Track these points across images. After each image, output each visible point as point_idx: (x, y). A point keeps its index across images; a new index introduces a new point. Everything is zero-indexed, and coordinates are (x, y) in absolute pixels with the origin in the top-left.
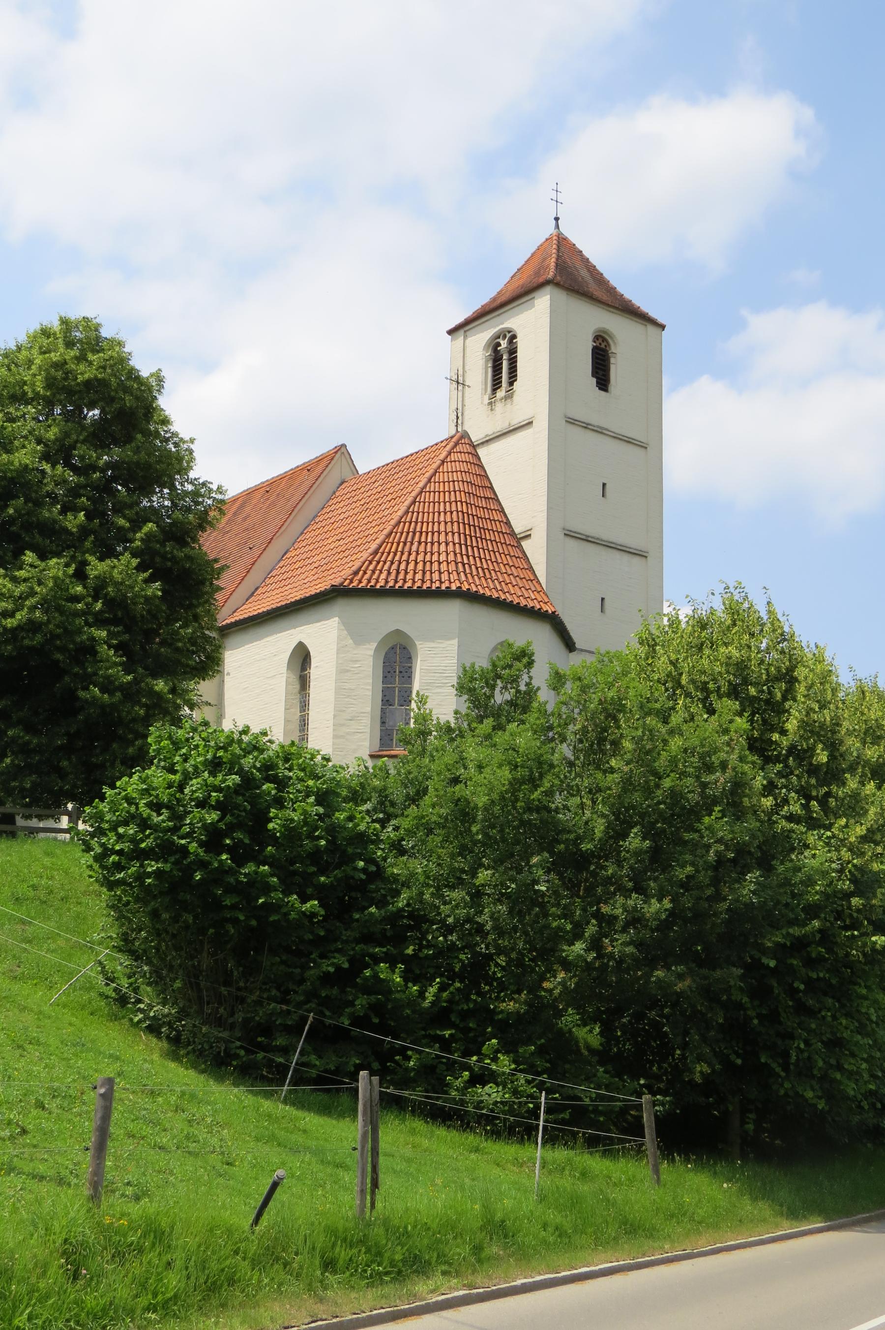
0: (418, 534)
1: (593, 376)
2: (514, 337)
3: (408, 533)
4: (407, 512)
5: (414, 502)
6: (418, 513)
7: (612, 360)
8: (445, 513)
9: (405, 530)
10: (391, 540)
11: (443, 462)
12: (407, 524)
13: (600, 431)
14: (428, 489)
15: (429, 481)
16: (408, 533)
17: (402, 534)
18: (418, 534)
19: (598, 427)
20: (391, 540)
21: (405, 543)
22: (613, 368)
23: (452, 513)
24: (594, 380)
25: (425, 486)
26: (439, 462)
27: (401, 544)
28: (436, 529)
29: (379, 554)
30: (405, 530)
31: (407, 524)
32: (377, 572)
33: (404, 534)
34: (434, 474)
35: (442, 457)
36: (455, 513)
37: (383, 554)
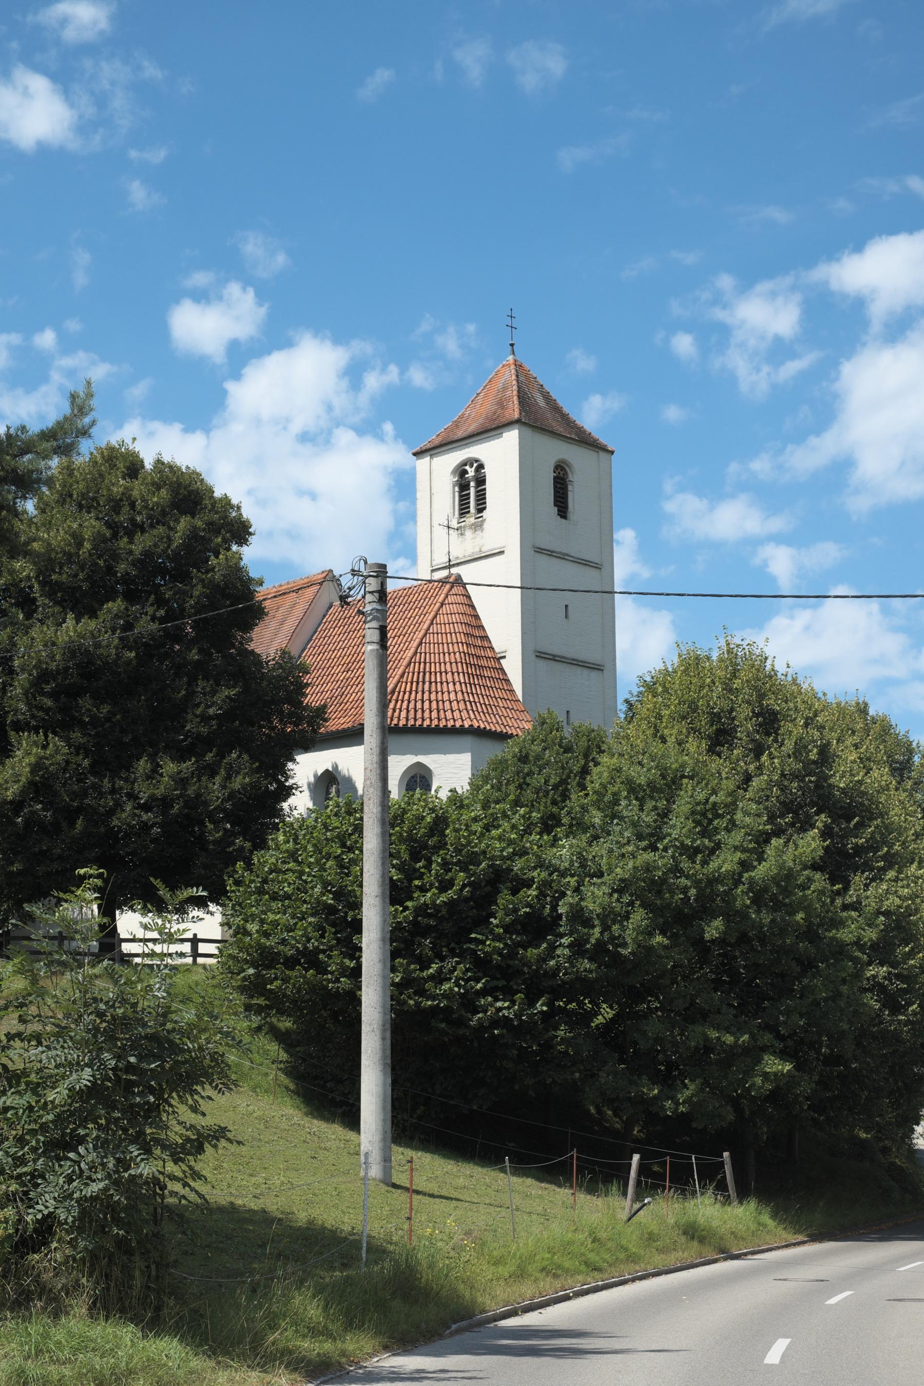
0: (427, 674)
1: (555, 505)
3: (419, 673)
4: (415, 653)
5: (420, 643)
6: (426, 653)
7: (570, 488)
9: (416, 670)
10: (404, 680)
12: (417, 664)
13: (563, 556)
14: (431, 631)
15: (432, 623)
16: (419, 673)
17: (413, 673)
18: (427, 674)
19: (560, 553)
20: (404, 680)
21: (418, 683)
22: (570, 494)
24: (556, 508)
25: (428, 629)
27: (414, 684)
28: (443, 670)
29: (396, 693)
30: (416, 670)
31: (417, 664)
32: (398, 711)
33: (416, 674)
34: (435, 617)
37: (399, 693)
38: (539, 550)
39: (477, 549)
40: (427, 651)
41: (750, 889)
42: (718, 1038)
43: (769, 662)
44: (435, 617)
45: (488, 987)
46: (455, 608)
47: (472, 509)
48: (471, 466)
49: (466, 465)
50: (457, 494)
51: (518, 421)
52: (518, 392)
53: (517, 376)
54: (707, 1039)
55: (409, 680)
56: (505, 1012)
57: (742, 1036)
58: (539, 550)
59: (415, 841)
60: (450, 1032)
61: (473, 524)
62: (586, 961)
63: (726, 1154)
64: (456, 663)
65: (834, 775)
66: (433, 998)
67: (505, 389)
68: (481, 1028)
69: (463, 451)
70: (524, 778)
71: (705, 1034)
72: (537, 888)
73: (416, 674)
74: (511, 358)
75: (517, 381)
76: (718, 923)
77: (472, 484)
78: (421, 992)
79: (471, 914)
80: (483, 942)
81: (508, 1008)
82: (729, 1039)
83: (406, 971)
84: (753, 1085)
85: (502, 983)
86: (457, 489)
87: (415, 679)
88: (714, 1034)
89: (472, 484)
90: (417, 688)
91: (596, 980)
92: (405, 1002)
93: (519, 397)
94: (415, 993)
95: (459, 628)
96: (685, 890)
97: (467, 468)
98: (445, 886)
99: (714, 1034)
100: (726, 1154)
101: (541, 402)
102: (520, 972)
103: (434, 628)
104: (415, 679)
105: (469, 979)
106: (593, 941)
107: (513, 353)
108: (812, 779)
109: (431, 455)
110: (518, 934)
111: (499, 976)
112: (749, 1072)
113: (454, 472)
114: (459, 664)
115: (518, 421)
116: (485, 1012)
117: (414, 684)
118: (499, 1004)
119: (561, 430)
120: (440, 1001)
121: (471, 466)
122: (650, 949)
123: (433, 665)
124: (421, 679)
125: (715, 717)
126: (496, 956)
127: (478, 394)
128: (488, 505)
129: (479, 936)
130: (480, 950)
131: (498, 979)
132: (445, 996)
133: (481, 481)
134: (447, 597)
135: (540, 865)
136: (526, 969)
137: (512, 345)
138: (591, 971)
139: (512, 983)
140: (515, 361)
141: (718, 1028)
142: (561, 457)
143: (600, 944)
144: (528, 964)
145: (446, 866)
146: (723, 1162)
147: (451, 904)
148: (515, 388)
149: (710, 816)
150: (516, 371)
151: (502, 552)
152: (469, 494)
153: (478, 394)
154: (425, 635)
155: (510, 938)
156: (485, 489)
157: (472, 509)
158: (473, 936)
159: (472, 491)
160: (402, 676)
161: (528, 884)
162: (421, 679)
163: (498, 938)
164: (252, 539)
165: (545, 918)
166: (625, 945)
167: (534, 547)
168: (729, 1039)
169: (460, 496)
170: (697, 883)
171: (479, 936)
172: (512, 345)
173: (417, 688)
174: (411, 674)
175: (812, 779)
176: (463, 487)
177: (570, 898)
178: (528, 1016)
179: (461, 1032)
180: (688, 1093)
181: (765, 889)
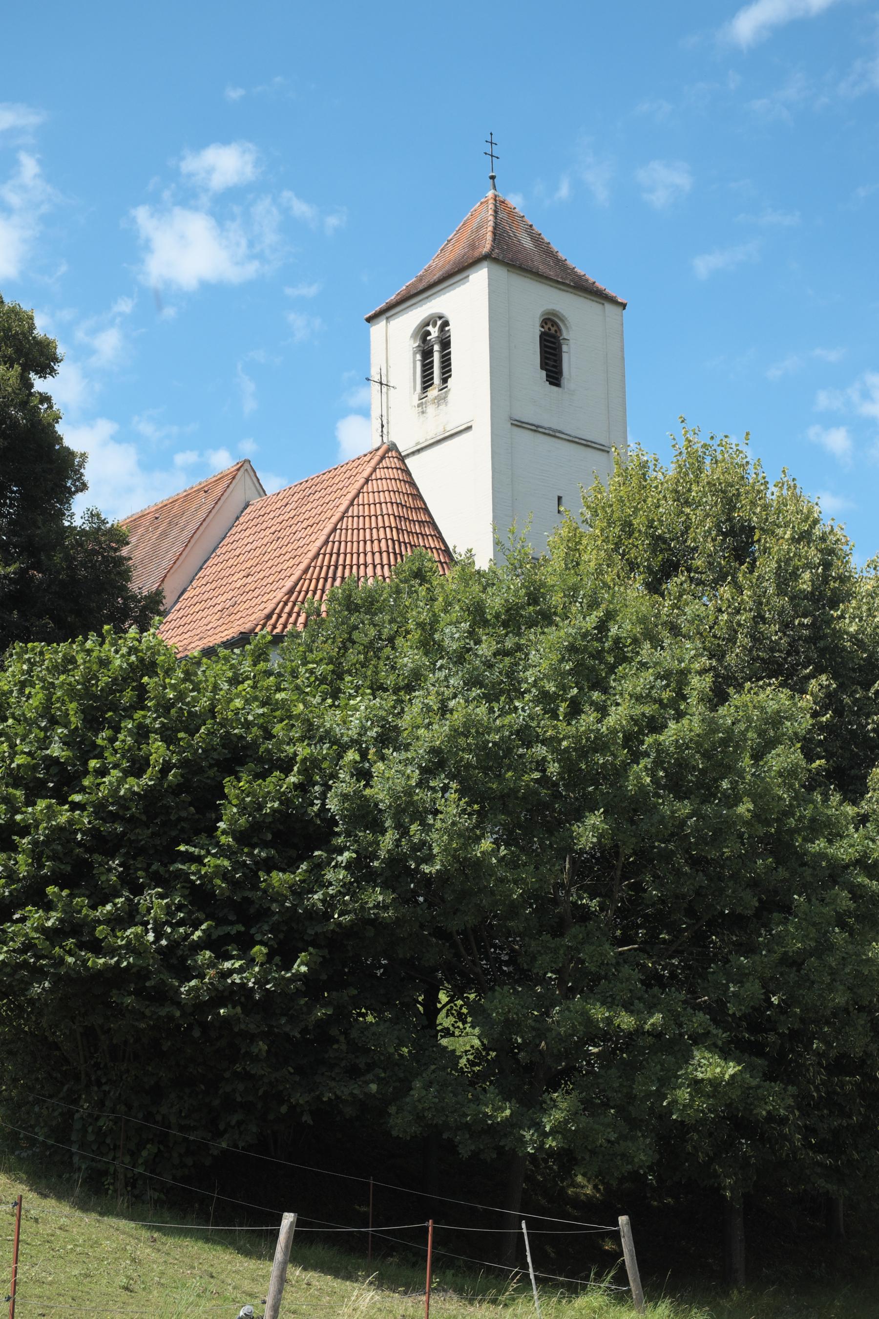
0: (340, 568)
1: (542, 368)
2: (446, 323)
3: (329, 567)
4: (326, 542)
5: (334, 530)
6: (340, 542)
8: (372, 542)
9: (326, 563)
10: (308, 576)
11: (367, 480)
12: (327, 556)
13: (553, 434)
14: (350, 513)
15: (351, 504)
16: (329, 567)
17: (321, 568)
18: (340, 568)
19: (550, 429)
20: (308, 576)
21: (326, 579)
22: (565, 357)
23: (379, 541)
24: (544, 373)
25: (347, 511)
26: (362, 481)
27: (321, 581)
28: (362, 561)
29: (295, 594)
30: (326, 563)
31: (327, 556)
32: (294, 615)
33: (325, 568)
34: (357, 496)
35: (366, 474)
36: (383, 541)
37: (300, 593)
38: (519, 424)
39: (441, 429)
40: (343, 539)
41: (658, 763)
42: (609, 1021)
43: (751, 469)
44: (357, 496)
45: (214, 937)
46: (383, 485)
47: (437, 380)
48: (435, 325)
49: (428, 325)
50: (419, 364)
51: (486, 257)
52: (495, 228)
53: (496, 212)
54: (589, 1021)
55: (315, 576)
56: (237, 978)
57: (651, 1015)
58: (519, 424)
59: (94, 697)
60: (148, 1012)
61: (435, 398)
62: (378, 889)
63: (623, 1220)
64: (381, 553)
65: (842, 617)
66: (112, 951)
67: (480, 227)
68: (200, 1007)
69: (425, 307)
70: (350, 633)
71: (585, 1014)
72: (299, 772)
73: (325, 568)
74: (490, 194)
75: (495, 217)
76: (595, 819)
77: (436, 348)
78: (96, 947)
79: (184, 814)
80: (199, 860)
81: (241, 970)
82: (626, 1021)
83: (69, 909)
84: (674, 1102)
85: (234, 930)
86: (419, 357)
87: (323, 575)
88: (599, 1013)
89: (436, 348)
90: (324, 586)
91: (399, 922)
92: (62, 961)
93: (494, 234)
94: (81, 946)
95: (387, 509)
96: (541, 766)
97: (430, 328)
98: (138, 767)
99: (599, 1013)
100: (623, 1220)
101: (527, 243)
102: (268, 912)
103: (354, 510)
104: (323, 575)
105: (181, 923)
106: (383, 854)
107: (495, 188)
108: (806, 621)
109: (387, 318)
110: (264, 845)
111: (232, 917)
112: (667, 1081)
113: (414, 336)
114: (385, 555)
115: (486, 257)
116: (201, 976)
117: (321, 581)
118: (227, 965)
119: (552, 274)
120: (121, 958)
121: (435, 325)
122: (478, 864)
123: (349, 556)
124: (330, 574)
125: (658, 542)
126: (218, 882)
127: (449, 241)
128: (453, 372)
129: (192, 849)
130: (194, 874)
131: (232, 923)
132: (129, 947)
133: (445, 344)
134: (374, 470)
135: (310, 734)
136: (275, 907)
137: (493, 178)
138: (385, 908)
139: (253, 931)
140: (496, 196)
141: (609, 1002)
142: (550, 307)
143: (396, 861)
144: (278, 898)
145: (142, 733)
146: (618, 1232)
147: (149, 796)
148: (491, 223)
149: (611, 660)
150: (496, 206)
151: (469, 428)
152: (432, 362)
153: (449, 241)
154: (342, 519)
155: (250, 855)
156: (449, 353)
157: (437, 380)
158: (182, 848)
159: (436, 357)
160: (306, 571)
161: (286, 766)
162: (330, 574)
163: (224, 851)
164: (59, 368)
165: (311, 821)
166: (429, 859)
167: (511, 419)
168: (626, 1021)
169: (423, 366)
170: (563, 757)
171: (192, 849)
172: (493, 178)
173: (324, 586)
174: (318, 569)
175: (806, 621)
176: (426, 354)
177: (345, 783)
178: (278, 982)
179: (163, 1012)
180: (558, 1115)
181: (683, 765)
